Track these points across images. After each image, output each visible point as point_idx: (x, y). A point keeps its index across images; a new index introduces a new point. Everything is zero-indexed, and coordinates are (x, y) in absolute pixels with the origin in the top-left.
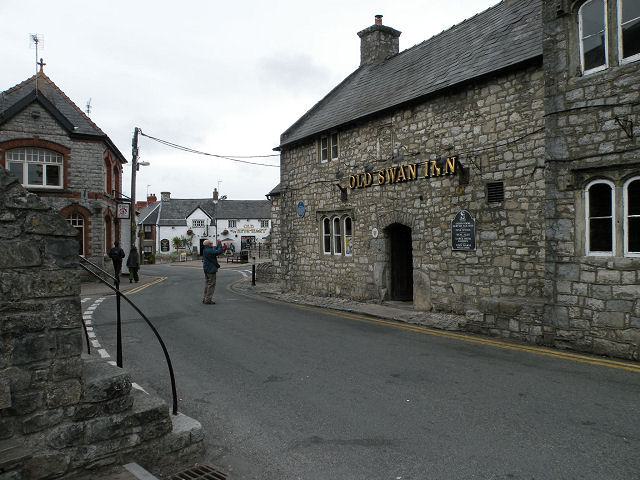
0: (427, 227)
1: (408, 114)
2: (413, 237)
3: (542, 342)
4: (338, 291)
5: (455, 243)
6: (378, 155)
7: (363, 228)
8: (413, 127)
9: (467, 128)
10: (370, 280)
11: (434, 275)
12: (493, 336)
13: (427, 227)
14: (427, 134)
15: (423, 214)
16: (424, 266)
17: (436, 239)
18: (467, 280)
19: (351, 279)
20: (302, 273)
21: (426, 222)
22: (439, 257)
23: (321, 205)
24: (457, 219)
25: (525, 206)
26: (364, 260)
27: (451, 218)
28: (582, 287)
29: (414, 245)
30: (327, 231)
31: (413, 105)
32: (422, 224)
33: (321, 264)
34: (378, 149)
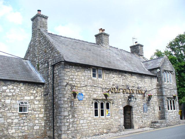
0: (137, 106)
1: (130, 75)
2: (133, 109)
3: (167, 126)
4: (105, 131)
5: (144, 110)
6: (121, 84)
7: (117, 107)
8: (132, 79)
9: (143, 84)
10: (119, 124)
11: (139, 119)
12: (161, 128)
13: (137, 106)
14: (136, 83)
15: (136, 103)
16: (137, 117)
17: (140, 110)
18: (145, 119)
19: (111, 125)
20: (81, 128)
21: (137, 105)
22: (140, 114)
23: (95, 96)
24: (144, 105)
25: (153, 103)
26: (117, 117)
27: (143, 104)
28: (169, 116)
29: (133, 111)
30: (96, 106)
31: (132, 73)
32: (136, 105)
33: (94, 122)
34: (121, 82)
